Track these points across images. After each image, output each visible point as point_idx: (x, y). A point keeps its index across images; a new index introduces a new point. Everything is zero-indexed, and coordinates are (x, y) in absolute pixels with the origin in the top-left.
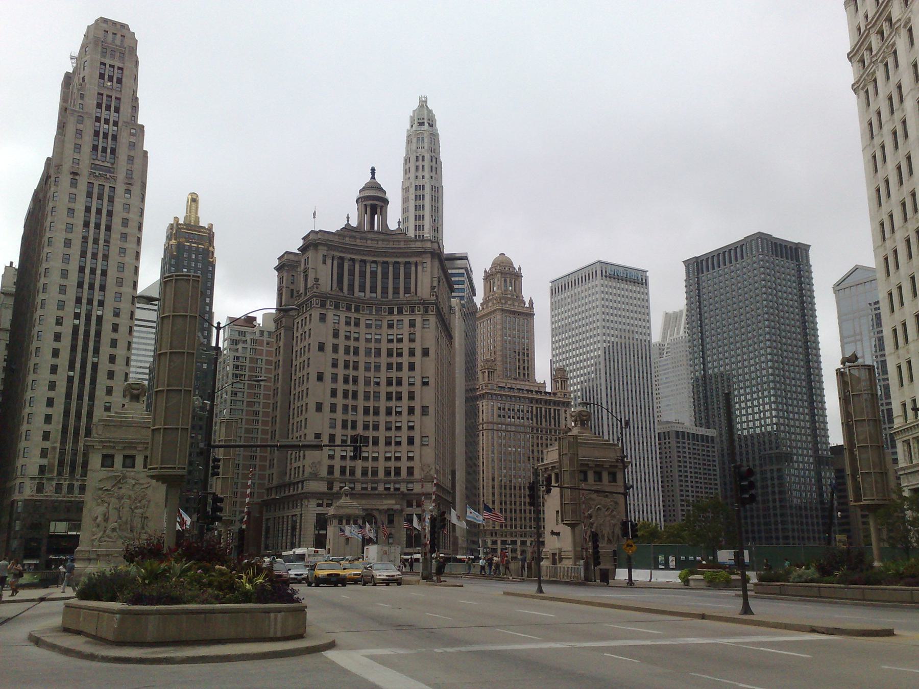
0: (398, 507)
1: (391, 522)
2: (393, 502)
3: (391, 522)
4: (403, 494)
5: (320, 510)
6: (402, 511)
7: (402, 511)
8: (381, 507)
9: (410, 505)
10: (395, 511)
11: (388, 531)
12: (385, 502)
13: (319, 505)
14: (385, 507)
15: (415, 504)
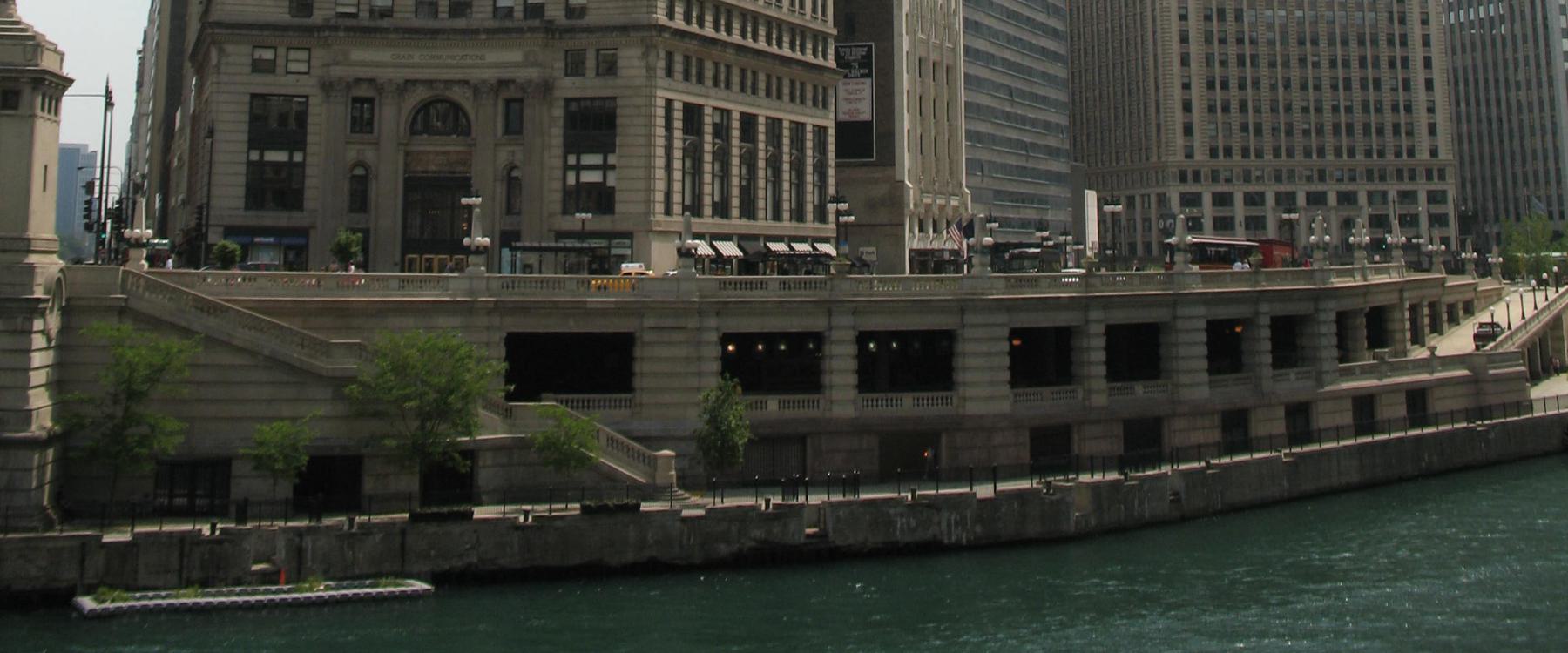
0: (533, 73)
1: (514, 127)
2: (515, 56)
3: (514, 127)
4: (550, 29)
5: (263, 83)
6: (546, 88)
7: (546, 88)
8: (476, 75)
9: (575, 66)
10: (522, 88)
11: (503, 157)
12: (492, 56)
13: (258, 67)
14: (490, 75)
15: (590, 63)
